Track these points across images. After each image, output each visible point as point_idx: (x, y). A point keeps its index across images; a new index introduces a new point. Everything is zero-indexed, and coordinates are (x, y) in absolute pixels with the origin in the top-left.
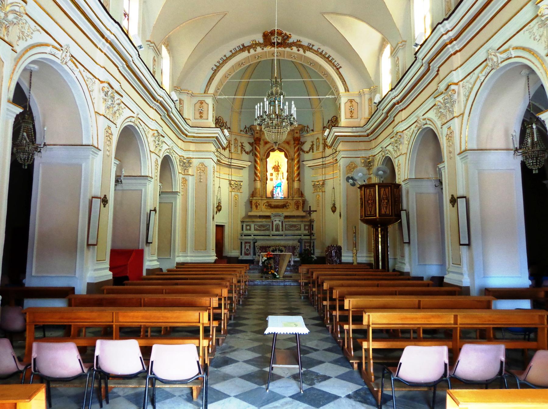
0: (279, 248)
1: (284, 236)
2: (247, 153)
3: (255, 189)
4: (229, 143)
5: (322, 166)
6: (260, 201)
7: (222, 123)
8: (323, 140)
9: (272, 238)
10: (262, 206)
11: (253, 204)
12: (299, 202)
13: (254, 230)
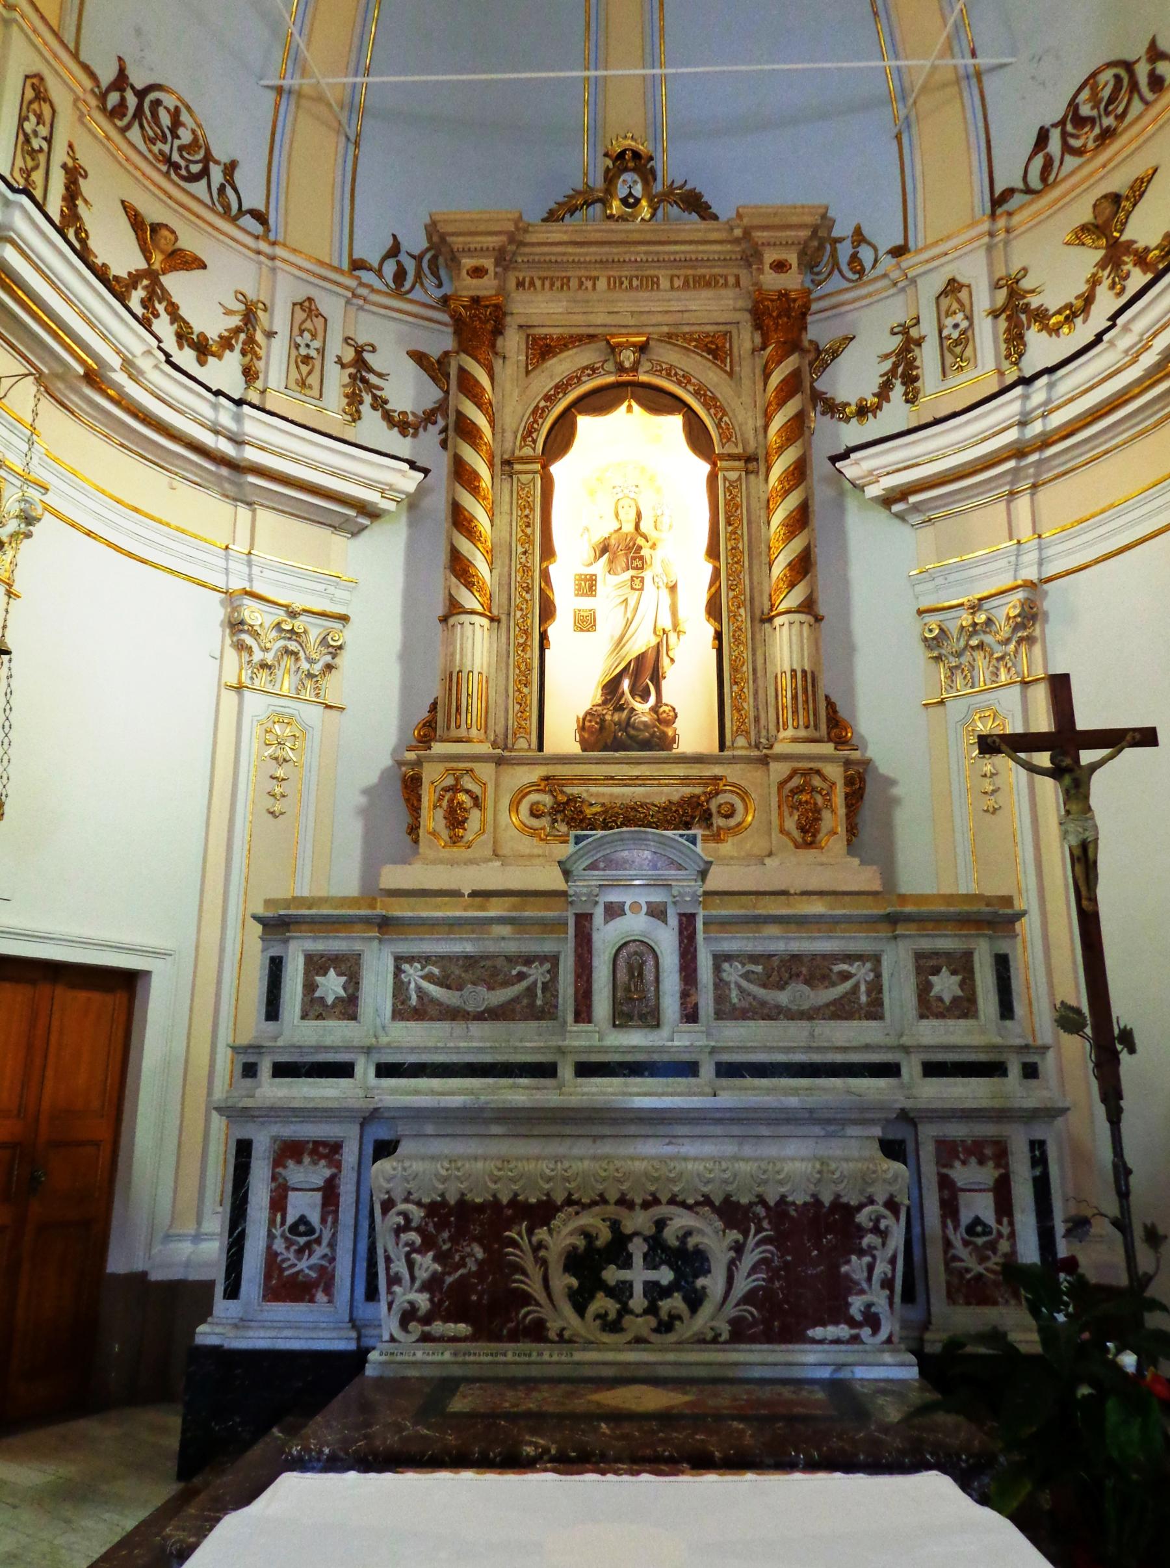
0: (661, 1224)
1: (707, 1070)
2: (402, 425)
3: (453, 679)
4: (249, 317)
5: (1015, 471)
6: (485, 771)
7: (181, 149)
8: (997, 286)
9: (574, 1101)
10: (504, 817)
11: (428, 797)
12: (817, 782)
13: (399, 1014)
